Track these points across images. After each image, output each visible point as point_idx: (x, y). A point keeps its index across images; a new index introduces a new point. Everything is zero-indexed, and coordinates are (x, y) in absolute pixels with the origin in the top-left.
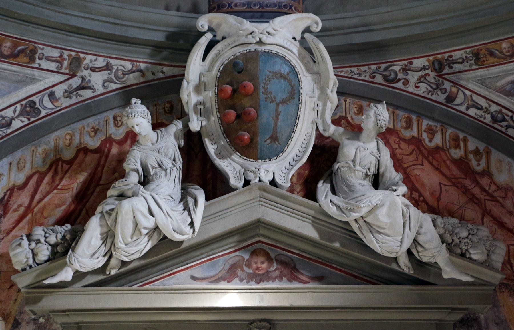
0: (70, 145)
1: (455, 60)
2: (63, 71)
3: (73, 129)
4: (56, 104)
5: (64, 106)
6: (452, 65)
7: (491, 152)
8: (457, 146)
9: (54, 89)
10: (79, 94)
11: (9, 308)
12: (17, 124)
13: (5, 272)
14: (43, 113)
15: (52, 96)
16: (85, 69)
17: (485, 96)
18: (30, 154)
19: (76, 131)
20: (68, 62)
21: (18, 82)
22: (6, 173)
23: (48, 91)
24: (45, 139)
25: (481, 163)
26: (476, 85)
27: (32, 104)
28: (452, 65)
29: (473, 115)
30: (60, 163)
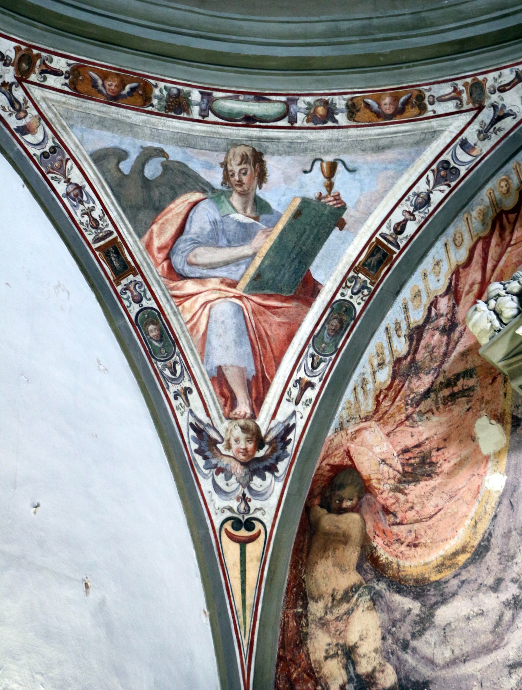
0: (508, 191)
2: (465, 107)
3: (507, 172)
4: (474, 153)
5: (485, 152)
9: (464, 136)
10: (497, 128)
11: (500, 406)
12: (436, 197)
13: (481, 366)
14: (463, 171)
15: (465, 145)
16: (492, 93)
18: (464, 223)
19: (511, 173)
20: (467, 93)
21: (417, 143)
22: (444, 256)
23: (457, 141)
24: (477, 199)
27: (445, 165)
30: (504, 216)
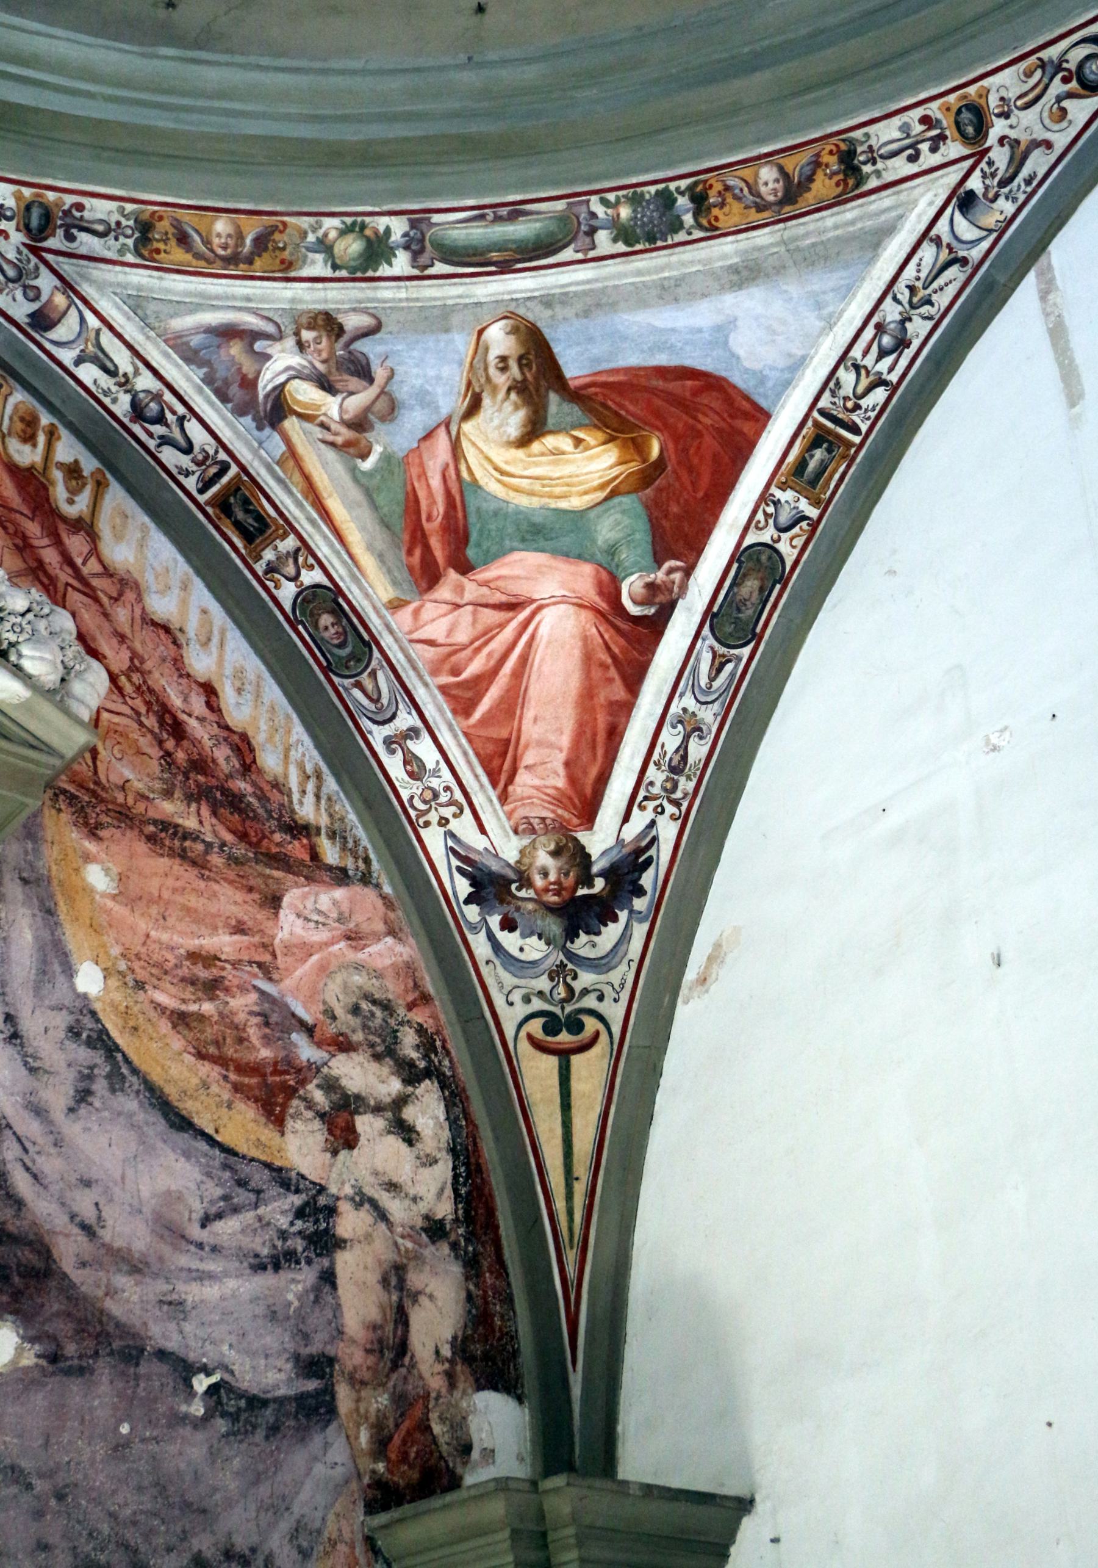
1: (88, 222)
6: (74, 231)
7: (107, 485)
8: (29, 438)
17: (132, 342)
25: (76, 499)
26: (119, 308)
28: (74, 231)
29: (88, 382)
